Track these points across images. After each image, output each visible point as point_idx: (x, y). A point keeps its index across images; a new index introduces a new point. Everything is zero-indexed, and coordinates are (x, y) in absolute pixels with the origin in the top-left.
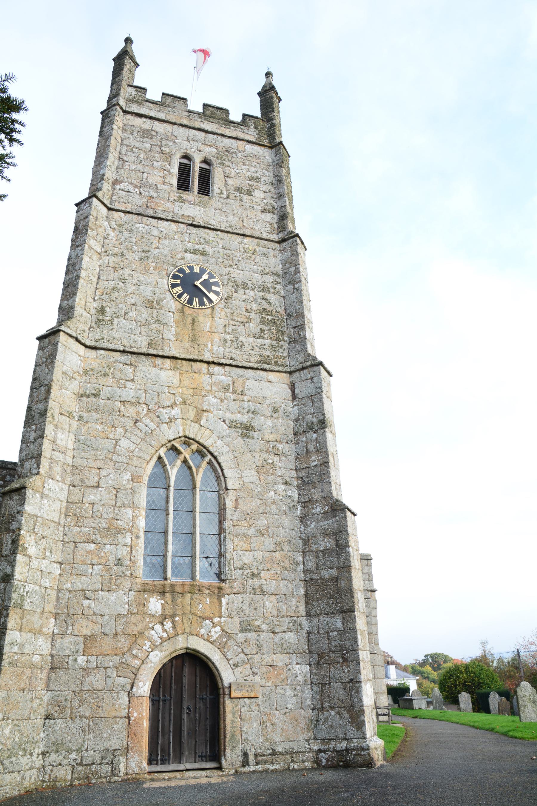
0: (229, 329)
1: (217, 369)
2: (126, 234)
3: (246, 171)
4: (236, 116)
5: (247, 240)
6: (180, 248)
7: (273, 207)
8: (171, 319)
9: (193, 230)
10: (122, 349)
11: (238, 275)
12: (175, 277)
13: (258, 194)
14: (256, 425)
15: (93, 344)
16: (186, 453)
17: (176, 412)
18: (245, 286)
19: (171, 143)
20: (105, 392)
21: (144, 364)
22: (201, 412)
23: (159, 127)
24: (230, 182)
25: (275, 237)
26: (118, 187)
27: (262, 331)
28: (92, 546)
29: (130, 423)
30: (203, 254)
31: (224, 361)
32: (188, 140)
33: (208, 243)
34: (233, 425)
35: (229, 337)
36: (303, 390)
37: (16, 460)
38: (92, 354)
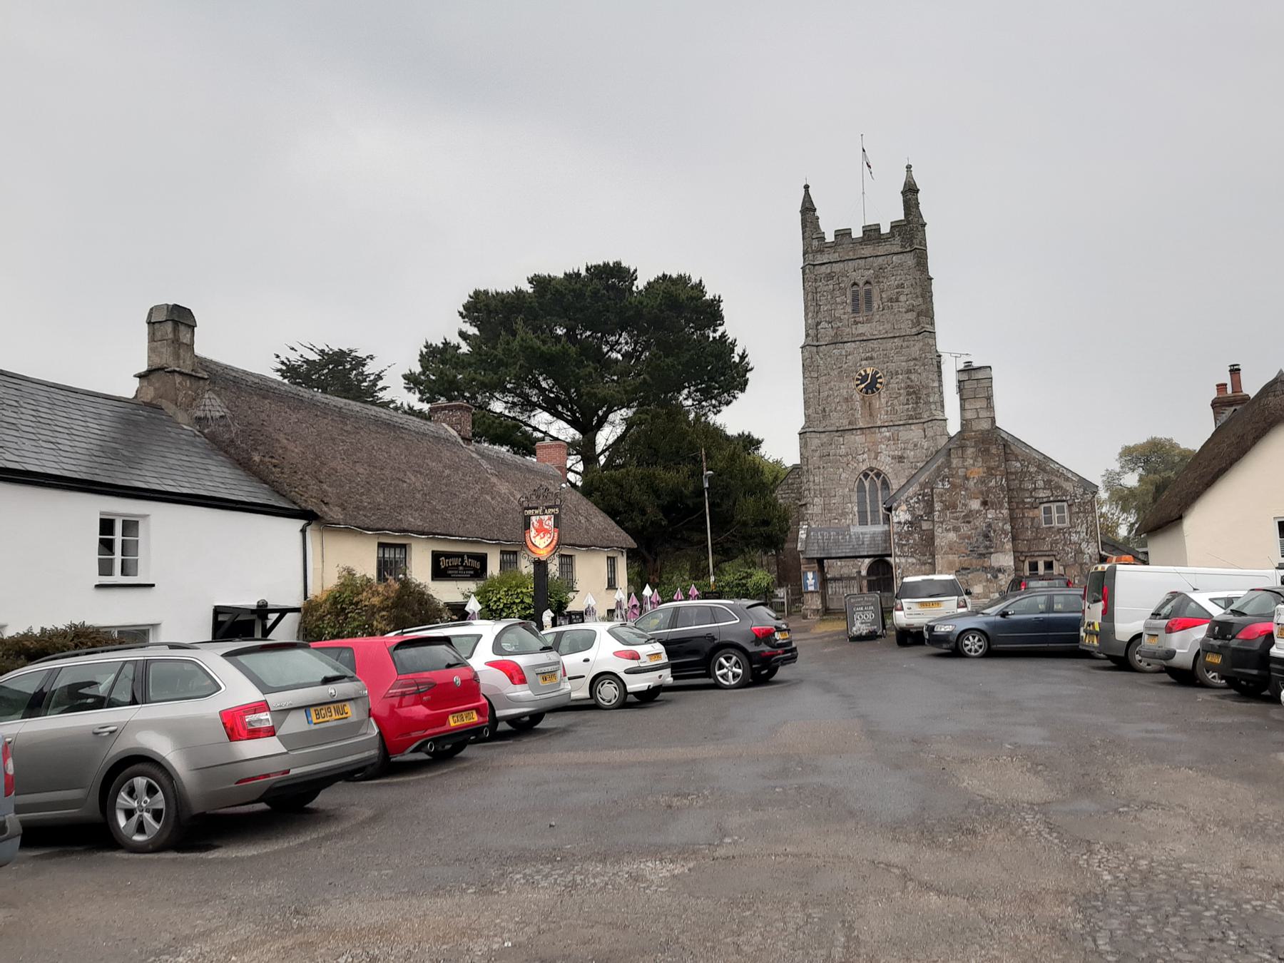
0: (889, 404)
1: (884, 429)
2: (829, 359)
3: (893, 282)
4: (885, 229)
5: (896, 340)
6: (858, 358)
7: (913, 306)
8: (858, 405)
10: (836, 429)
11: (892, 367)
12: (858, 379)
13: (902, 298)
14: (905, 455)
15: (823, 430)
16: (871, 474)
17: (865, 456)
18: (897, 373)
19: (844, 279)
20: (832, 452)
21: (848, 436)
22: (877, 454)
23: (837, 268)
24: (884, 296)
25: (914, 331)
26: (819, 327)
27: (908, 400)
28: (837, 521)
29: (845, 465)
31: (886, 424)
32: (855, 271)
33: (873, 350)
34: (893, 458)
35: (889, 408)
36: (930, 433)
38: (823, 435)
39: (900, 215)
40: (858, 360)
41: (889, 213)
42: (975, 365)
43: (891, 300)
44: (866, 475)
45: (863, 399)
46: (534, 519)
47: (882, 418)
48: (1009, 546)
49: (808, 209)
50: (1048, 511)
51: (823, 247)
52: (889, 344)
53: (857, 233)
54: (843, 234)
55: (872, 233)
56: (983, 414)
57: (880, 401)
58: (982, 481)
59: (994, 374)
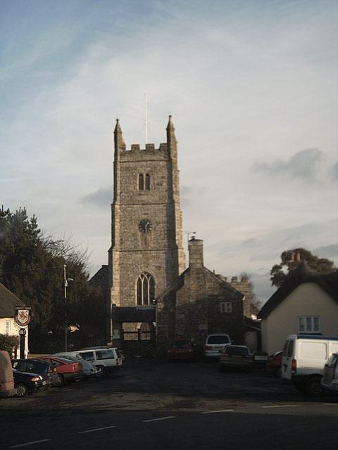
8: (139, 238)
9: (144, 206)
17: (142, 265)
21: (133, 254)
23: (131, 165)
24: (156, 182)
30: (147, 214)
34: (156, 267)
37: (107, 264)
39: (165, 141)
40: (139, 213)
41: (159, 139)
42: (196, 238)
43: (158, 184)
44: (142, 276)
45: (142, 235)
46: (20, 311)
47: (152, 245)
48: (206, 321)
49: (117, 132)
50: (223, 306)
51: (124, 153)
52: (156, 207)
53: (143, 147)
54: (135, 147)
55: (150, 148)
56: (199, 261)
57: (151, 237)
58: (197, 291)
59: (204, 243)
